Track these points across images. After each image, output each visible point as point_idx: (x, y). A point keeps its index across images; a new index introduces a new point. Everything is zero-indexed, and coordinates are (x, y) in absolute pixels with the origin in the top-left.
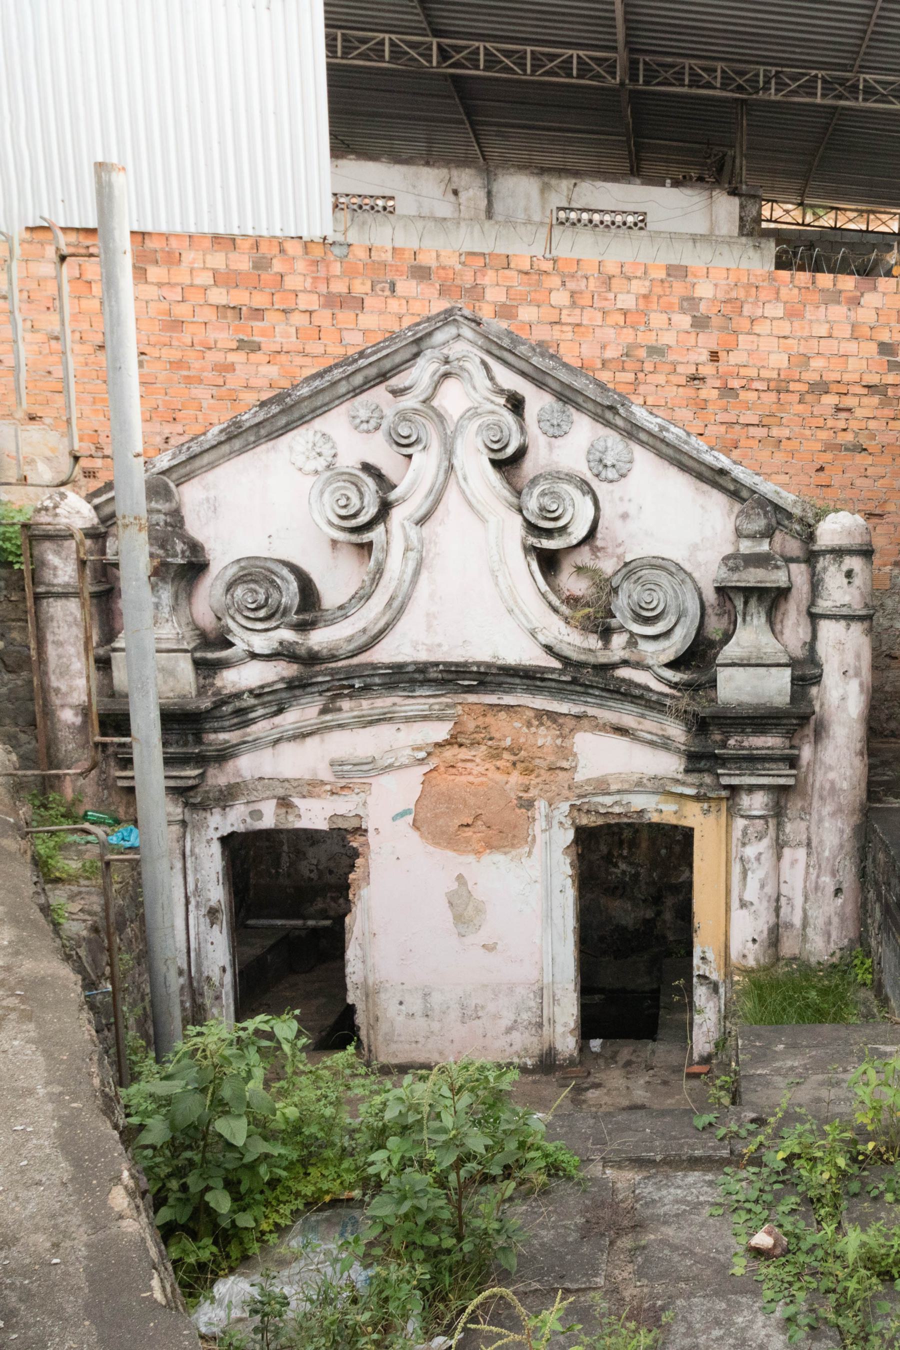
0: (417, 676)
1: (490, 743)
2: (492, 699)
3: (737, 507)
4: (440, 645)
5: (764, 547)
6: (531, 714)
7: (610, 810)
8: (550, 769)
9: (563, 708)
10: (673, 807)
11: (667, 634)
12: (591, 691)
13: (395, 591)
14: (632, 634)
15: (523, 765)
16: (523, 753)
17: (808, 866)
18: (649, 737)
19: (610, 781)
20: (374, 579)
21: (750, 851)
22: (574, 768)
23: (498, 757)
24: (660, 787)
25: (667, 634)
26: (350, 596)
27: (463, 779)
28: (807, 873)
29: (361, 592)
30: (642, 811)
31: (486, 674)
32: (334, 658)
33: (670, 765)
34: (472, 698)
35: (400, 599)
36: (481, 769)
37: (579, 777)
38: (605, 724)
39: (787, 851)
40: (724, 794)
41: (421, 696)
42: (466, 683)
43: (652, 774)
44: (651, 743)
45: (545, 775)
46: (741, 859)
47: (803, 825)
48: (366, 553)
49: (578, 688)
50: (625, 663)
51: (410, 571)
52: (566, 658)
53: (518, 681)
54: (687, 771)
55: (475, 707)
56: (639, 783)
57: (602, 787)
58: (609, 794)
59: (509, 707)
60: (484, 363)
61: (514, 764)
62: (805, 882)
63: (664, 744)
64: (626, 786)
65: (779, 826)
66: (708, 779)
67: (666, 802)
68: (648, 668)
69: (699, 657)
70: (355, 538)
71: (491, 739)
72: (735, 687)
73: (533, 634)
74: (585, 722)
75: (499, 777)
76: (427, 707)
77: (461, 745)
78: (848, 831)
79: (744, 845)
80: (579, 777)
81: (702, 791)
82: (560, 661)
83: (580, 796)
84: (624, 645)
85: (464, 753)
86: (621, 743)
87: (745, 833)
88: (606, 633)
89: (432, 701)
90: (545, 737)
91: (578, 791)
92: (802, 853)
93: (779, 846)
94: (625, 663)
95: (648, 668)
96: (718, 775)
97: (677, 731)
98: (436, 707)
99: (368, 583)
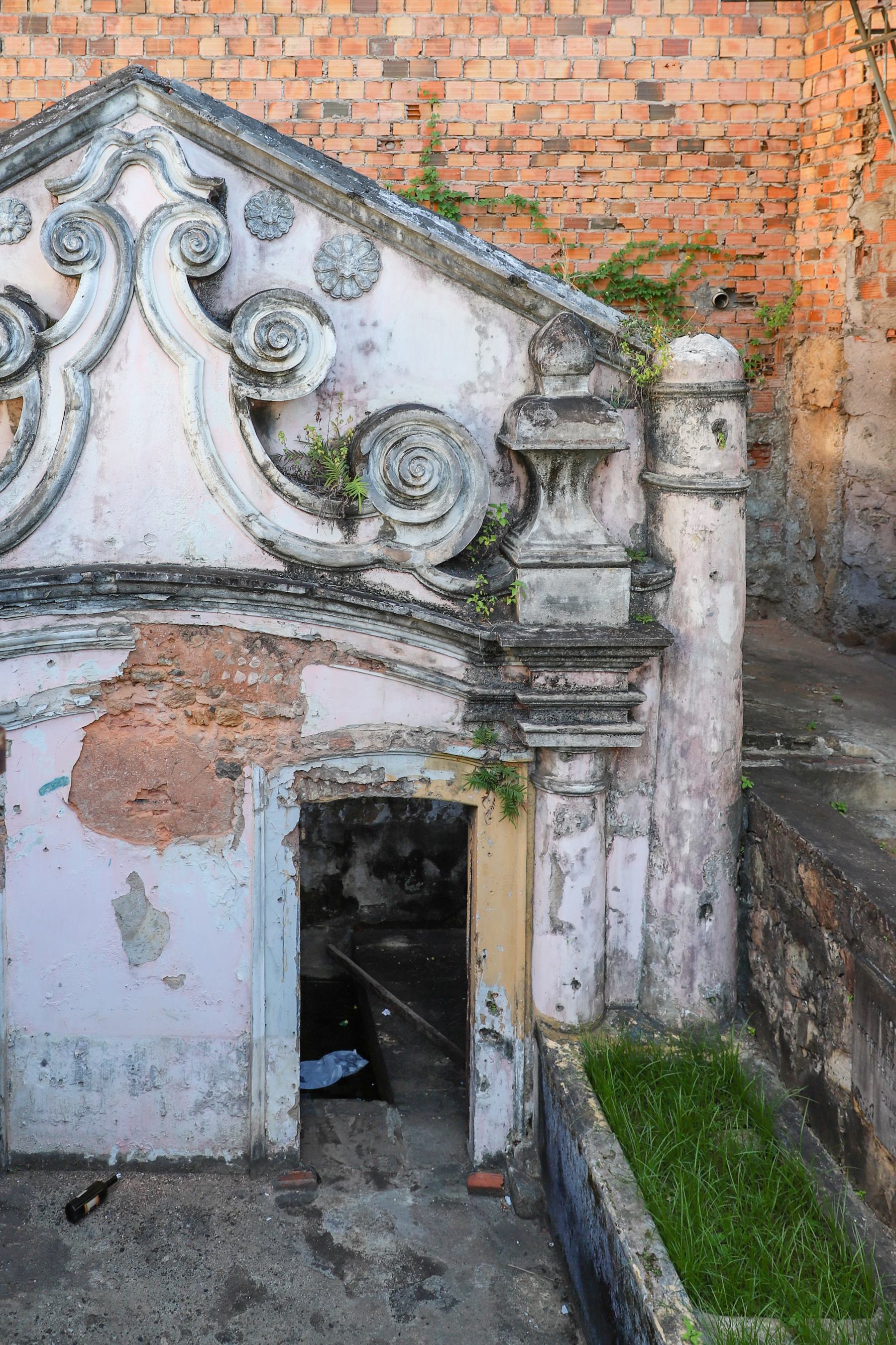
1: (178, 680)
3: (532, 327)
5: (584, 388)
6: (239, 638)
7: (353, 779)
8: (266, 718)
10: (448, 775)
11: (439, 520)
14: (387, 521)
15: (227, 711)
16: (224, 694)
17: (651, 864)
18: (414, 673)
19: (355, 736)
21: (568, 847)
22: (300, 718)
23: (189, 699)
24: (427, 743)
25: (439, 520)
27: (141, 733)
28: (650, 877)
30: (400, 781)
33: (441, 711)
36: (165, 717)
37: (309, 730)
38: (347, 653)
39: (619, 843)
40: (526, 756)
43: (415, 724)
44: (418, 682)
45: (260, 729)
46: (554, 857)
47: (643, 803)
54: (465, 722)
56: (397, 736)
57: (342, 743)
58: (353, 756)
61: (213, 710)
62: (648, 889)
63: (437, 680)
64: (379, 744)
65: (609, 803)
66: (500, 732)
67: (437, 767)
68: (412, 570)
69: (482, 557)
71: (180, 674)
72: (537, 599)
74: (317, 649)
75: (194, 731)
77: (135, 683)
78: (719, 818)
79: (558, 835)
80: (309, 730)
81: (492, 753)
83: (309, 759)
84: (374, 536)
85: (142, 694)
86: (370, 682)
87: (560, 818)
90: (255, 672)
91: (307, 751)
92: (641, 845)
93: (609, 832)
95: (412, 570)
96: (519, 729)
97: (451, 661)
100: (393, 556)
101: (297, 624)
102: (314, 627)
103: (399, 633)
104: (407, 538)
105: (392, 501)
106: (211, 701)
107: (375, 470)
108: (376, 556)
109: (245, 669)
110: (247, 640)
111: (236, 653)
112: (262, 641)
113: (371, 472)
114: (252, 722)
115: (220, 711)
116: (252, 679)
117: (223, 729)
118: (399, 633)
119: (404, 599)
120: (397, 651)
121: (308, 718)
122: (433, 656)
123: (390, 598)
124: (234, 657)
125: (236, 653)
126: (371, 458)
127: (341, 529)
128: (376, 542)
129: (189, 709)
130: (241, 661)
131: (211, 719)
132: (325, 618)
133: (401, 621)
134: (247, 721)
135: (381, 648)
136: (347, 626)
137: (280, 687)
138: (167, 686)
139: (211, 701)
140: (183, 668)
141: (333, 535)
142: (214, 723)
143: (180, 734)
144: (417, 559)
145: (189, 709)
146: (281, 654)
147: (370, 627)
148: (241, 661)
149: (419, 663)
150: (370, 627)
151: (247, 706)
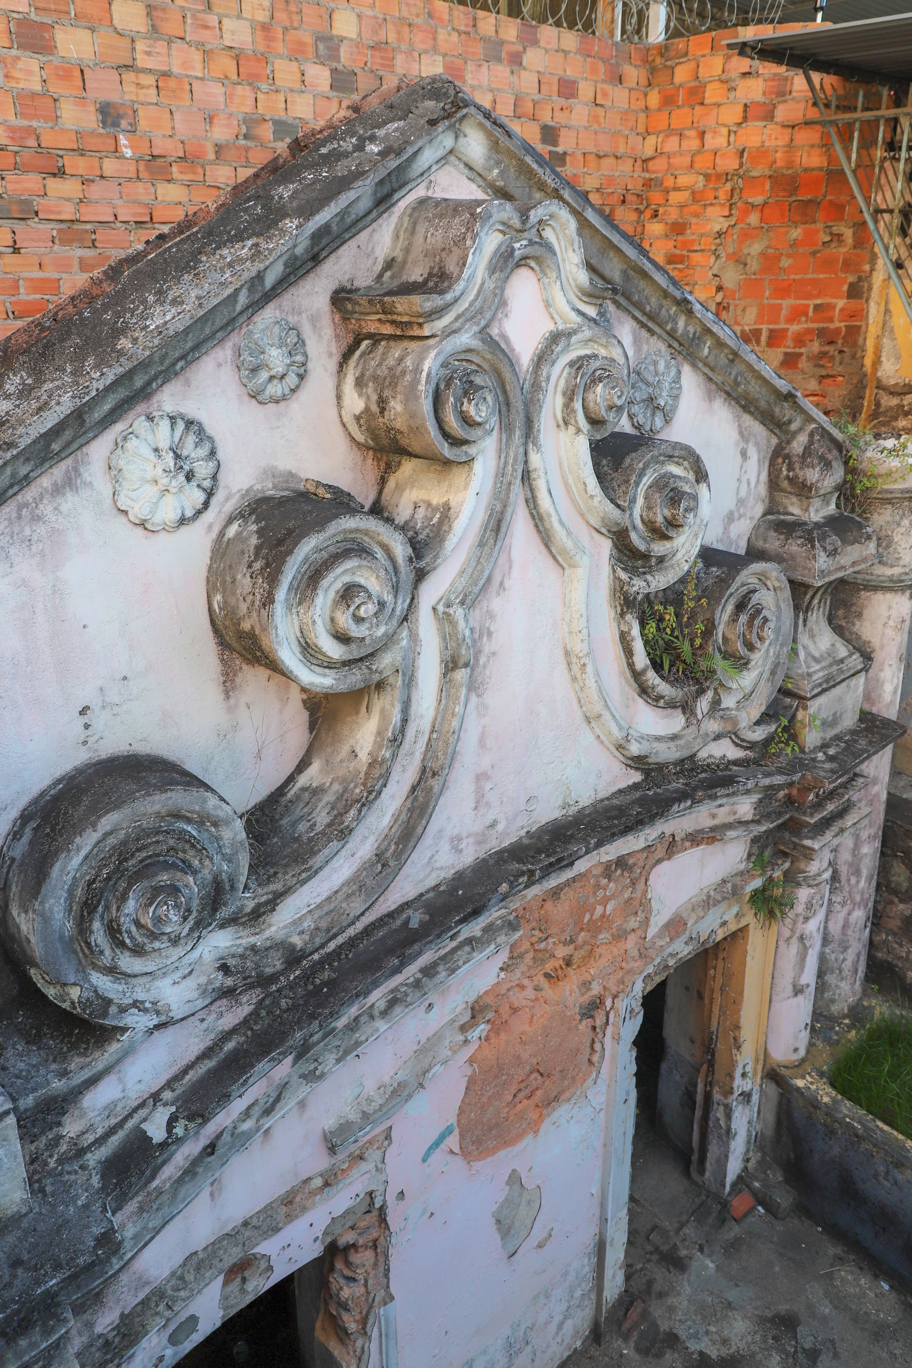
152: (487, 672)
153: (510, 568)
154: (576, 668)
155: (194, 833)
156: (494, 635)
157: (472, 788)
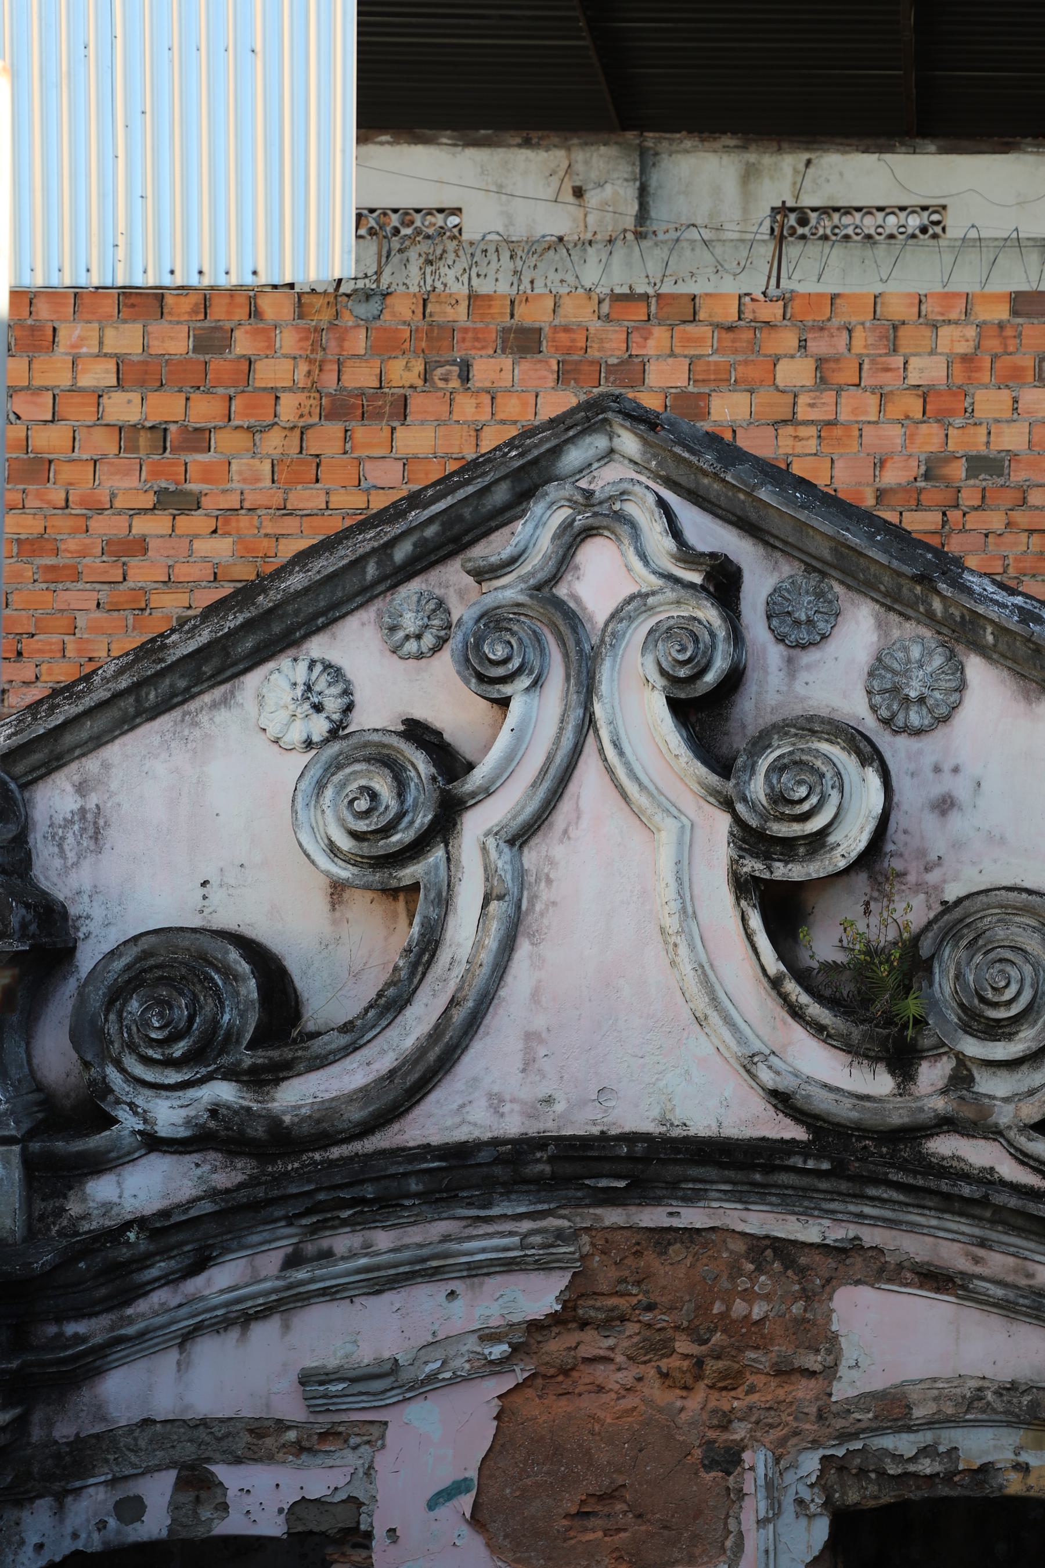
0: (498, 1170)
1: (647, 1317)
2: (653, 1217)
4: (549, 1101)
6: (739, 1246)
9: (809, 1231)
12: (872, 1191)
13: (460, 989)
14: (961, 1060)
18: (999, 1292)
20: (414, 966)
22: (830, 1372)
26: (365, 1004)
29: (391, 992)
31: (645, 1160)
32: (325, 1139)
34: (613, 1216)
35: (470, 1004)
38: (900, 1266)
41: (504, 1217)
42: (603, 1183)
44: (1007, 1308)
48: (401, 906)
49: (844, 1186)
50: (947, 1124)
51: (492, 942)
52: (817, 1117)
53: (712, 1172)
55: (618, 1236)
59: (692, 1233)
60: (661, 503)
70: (376, 877)
71: (650, 1307)
73: (749, 1065)
74: (857, 1261)
76: (516, 1239)
82: (809, 1128)
84: (941, 1084)
86: (932, 1311)
88: (901, 1058)
89: (526, 1225)
94: (947, 1124)
98: (537, 1239)
99: (403, 974)
100: (967, 1113)
101: (827, 1222)
102: (852, 1226)
103: (977, 1231)
104: (992, 1085)
105: (968, 1030)
106: (695, 1349)
107: (944, 985)
108: (942, 1112)
109: (748, 1296)
110: (751, 1249)
111: (735, 1271)
112: (775, 1250)
113: (937, 985)
114: (759, 1380)
115: (712, 1366)
116: (758, 1311)
117: (715, 1394)
118: (977, 1231)
119: (987, 1179)
120: (977, 1260)
121: (842, 1371)
122: (1031, 1267)
123: (965, 1176)
124: (732, 1278)
125: (735, 1271)
126: (936, 965)
127: (892, 1072)
128: (944, 1092)
129: (664, 1364)
130: (743, 1283)
131: (698, 1378)
132: (868, 1210)
133: (977, 1211)
134: (751, 1379)
135: (953, 1255)
136: (901, 1222)
137: (800, 1322)
138: (632, 1328)
139: (695, 1349)
140: (655, 1297)
141: (881, 1083)
142: (701, 1385)
143: (648, 1402)
144: (1004, 1116)
145: (664, 1364)
146: (803, 1272)
147: (934, 1222)
148: (743, 1283)
149: (1010, 1279)
150: (934, 1222)
151: (752, 1355)
152: (546, 921)
153: (578, 818)
154: (671, 947)
155: (220, 983)
156: (555, 884)
157: (520, 1045)
